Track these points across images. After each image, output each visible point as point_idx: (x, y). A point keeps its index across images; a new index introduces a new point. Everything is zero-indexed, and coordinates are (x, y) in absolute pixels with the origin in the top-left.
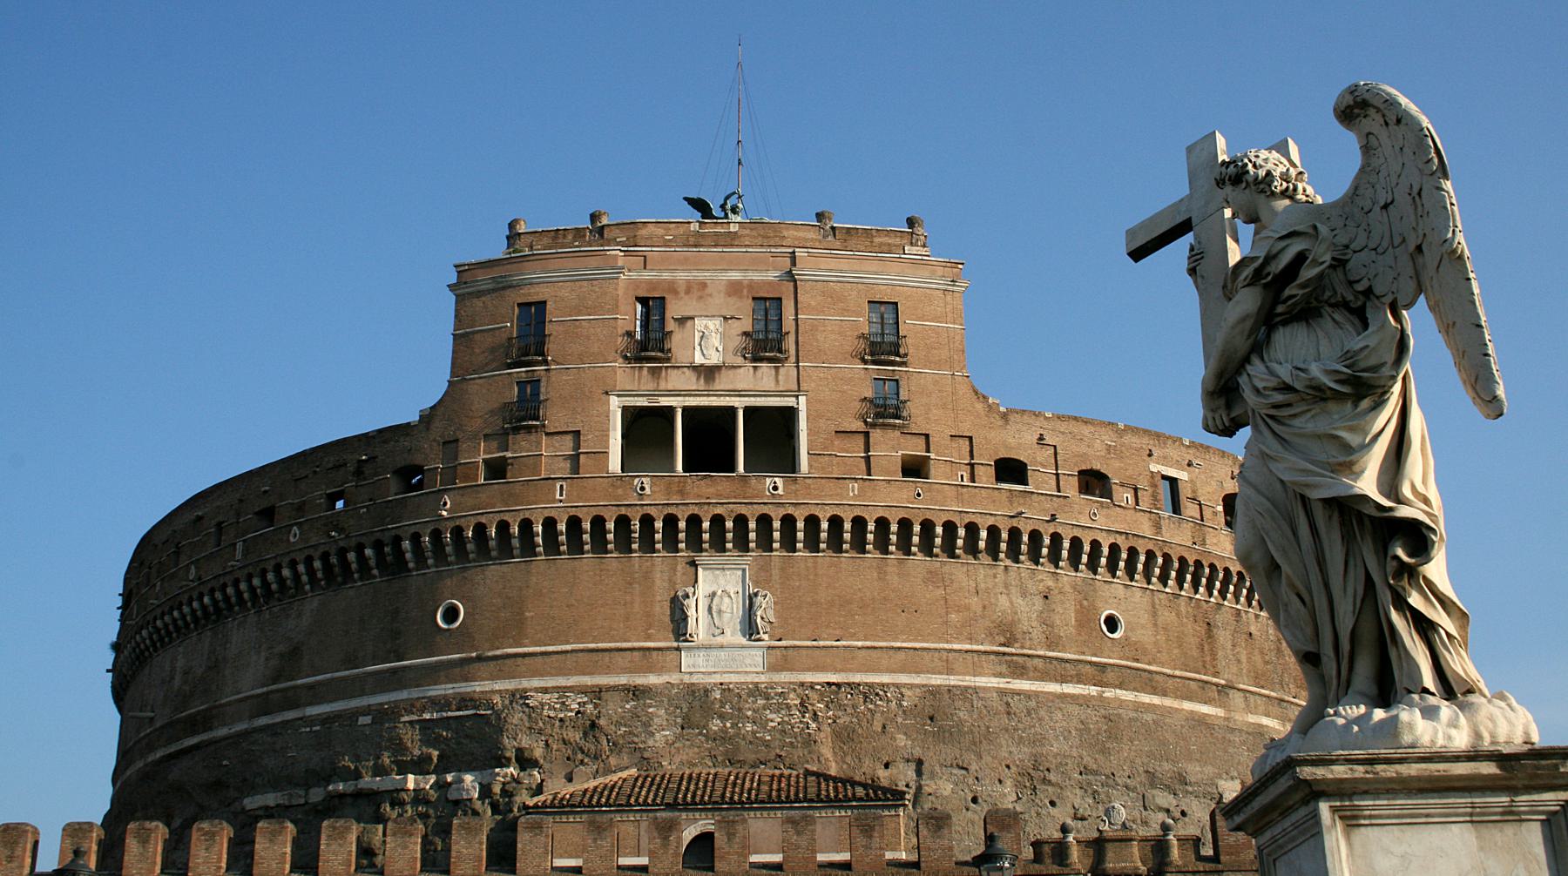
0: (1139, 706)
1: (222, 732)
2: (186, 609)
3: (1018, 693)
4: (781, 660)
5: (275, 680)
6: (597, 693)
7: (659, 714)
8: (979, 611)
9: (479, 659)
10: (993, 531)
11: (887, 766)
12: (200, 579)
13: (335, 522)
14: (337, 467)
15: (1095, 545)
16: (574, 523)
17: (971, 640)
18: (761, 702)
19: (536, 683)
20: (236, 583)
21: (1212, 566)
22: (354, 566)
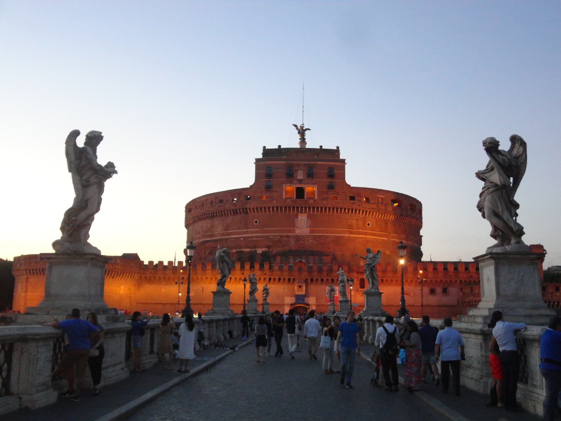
0: (372, 238)
1: (216, 238)
2: (206, 216)
4: (312, 231)
5: (225, 230)
6: (281, 236)
7: (292, 240)
10: (349, 210)
11: (329, 249)
12: (208, 211)
13: (235, 205)
16: (277, 208)
17: (344, 228)
18: (309, 238)
20: (216, 212)
22: (239, 212)
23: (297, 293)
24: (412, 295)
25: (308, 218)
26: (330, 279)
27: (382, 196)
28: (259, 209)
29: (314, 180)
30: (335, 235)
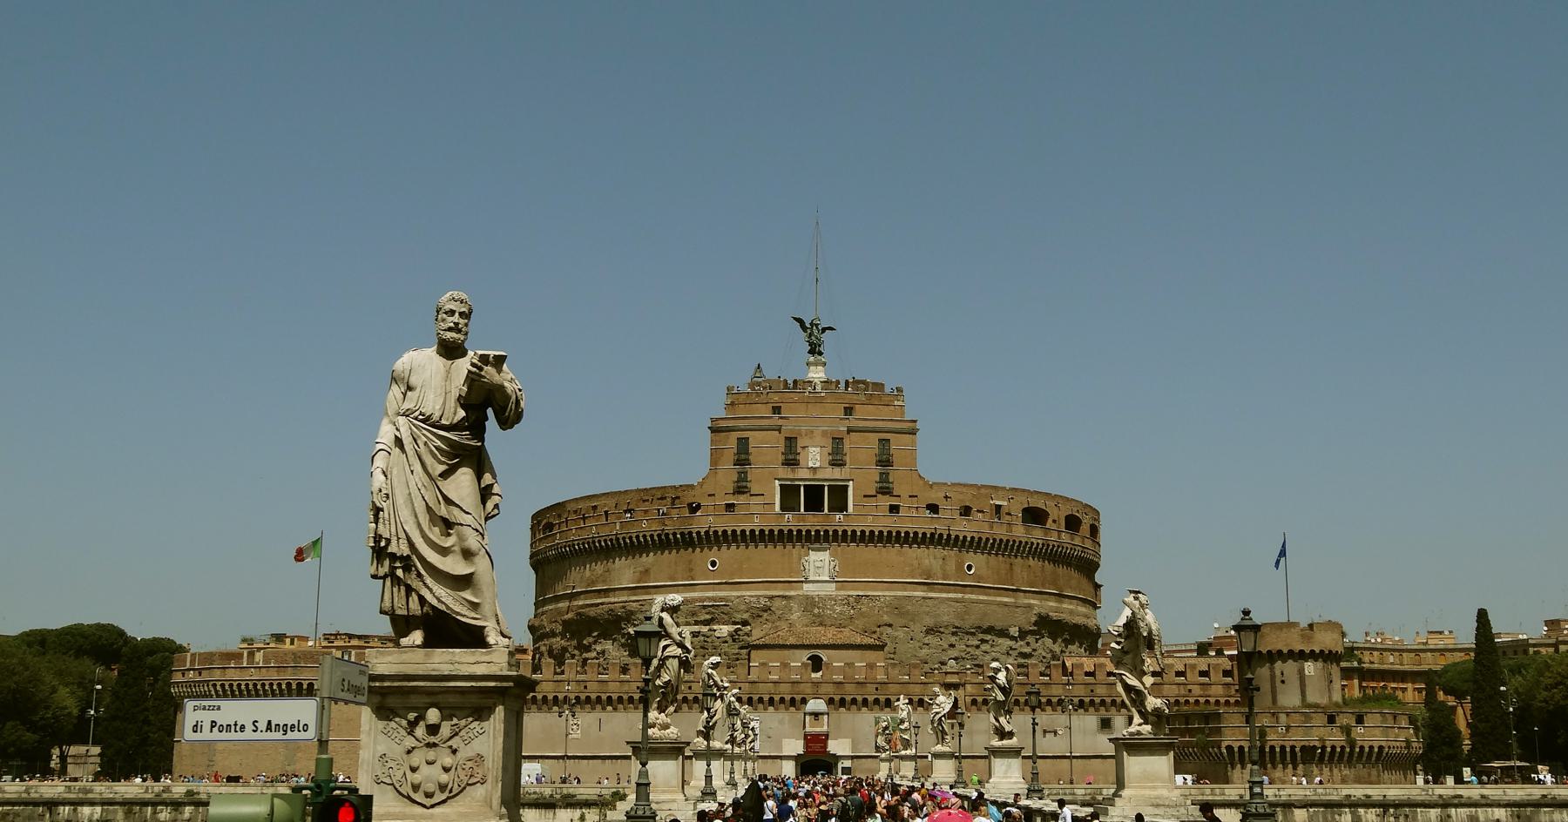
1: (616, 600)
3: (931, 598)
6: (771, 598)
8: (917, 566)
9: (726, 583)
11: (879, 627)
14: (662, 499)
15: (965, 537)
16: (762, 531)
17: (913, 578)
18: (833, 602)
19: (748, 593)
21: (1014, 541)
23: (808, 729)
24: (1060, 732)
25: (831, 555)
26: (882, 698)
27: (998, 503)
28: (720, 533)
29: (846, 469)
30: (892, 593)
